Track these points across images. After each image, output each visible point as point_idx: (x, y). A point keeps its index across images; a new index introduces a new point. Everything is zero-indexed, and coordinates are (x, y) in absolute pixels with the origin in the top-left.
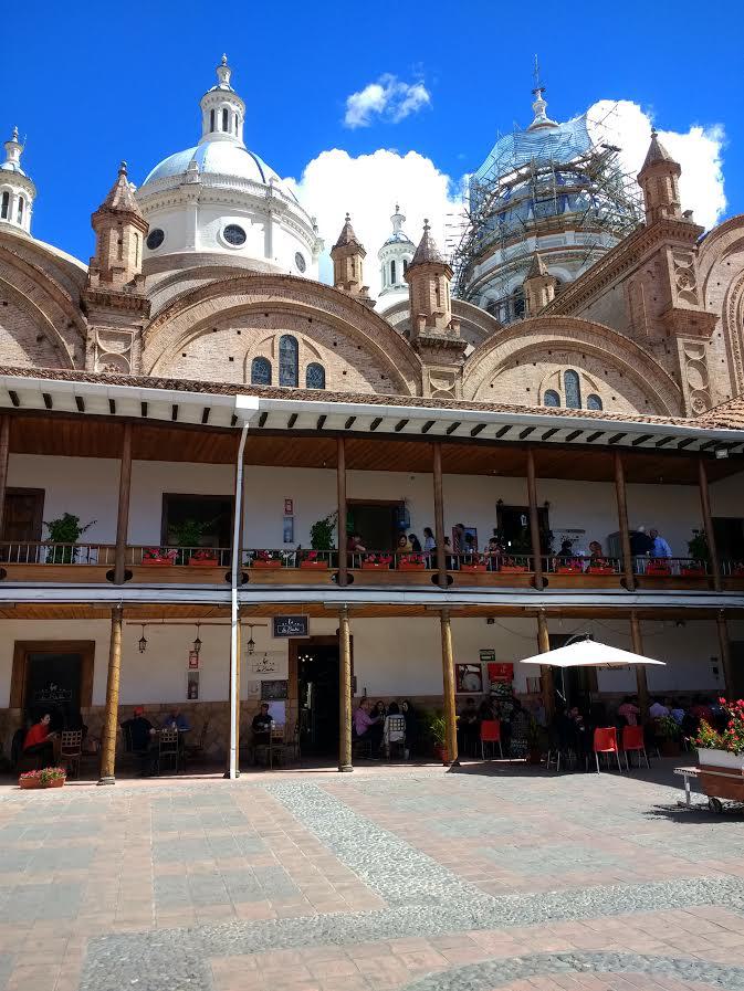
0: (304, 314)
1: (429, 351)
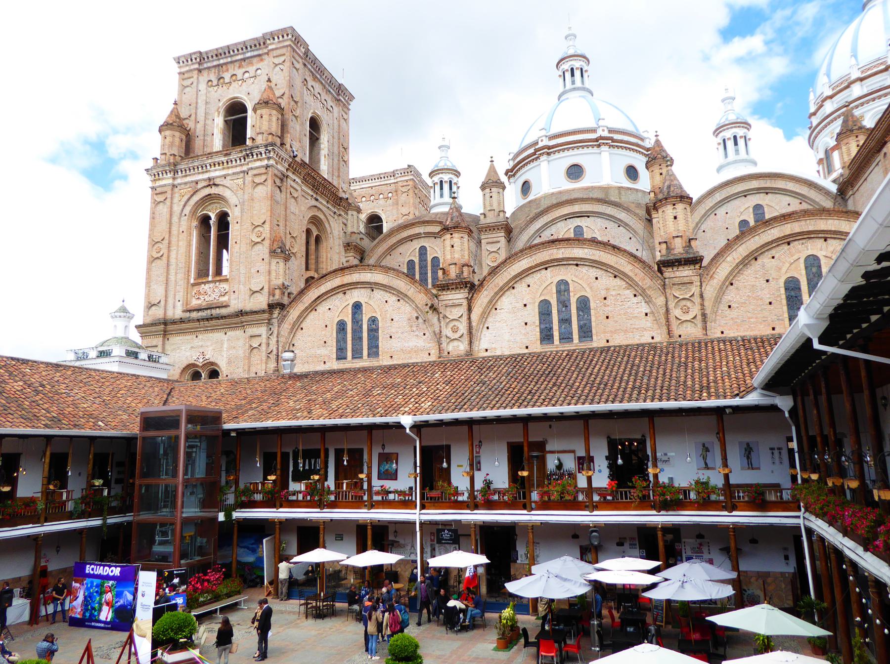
0: (572, 262)
1: (670, 269)
